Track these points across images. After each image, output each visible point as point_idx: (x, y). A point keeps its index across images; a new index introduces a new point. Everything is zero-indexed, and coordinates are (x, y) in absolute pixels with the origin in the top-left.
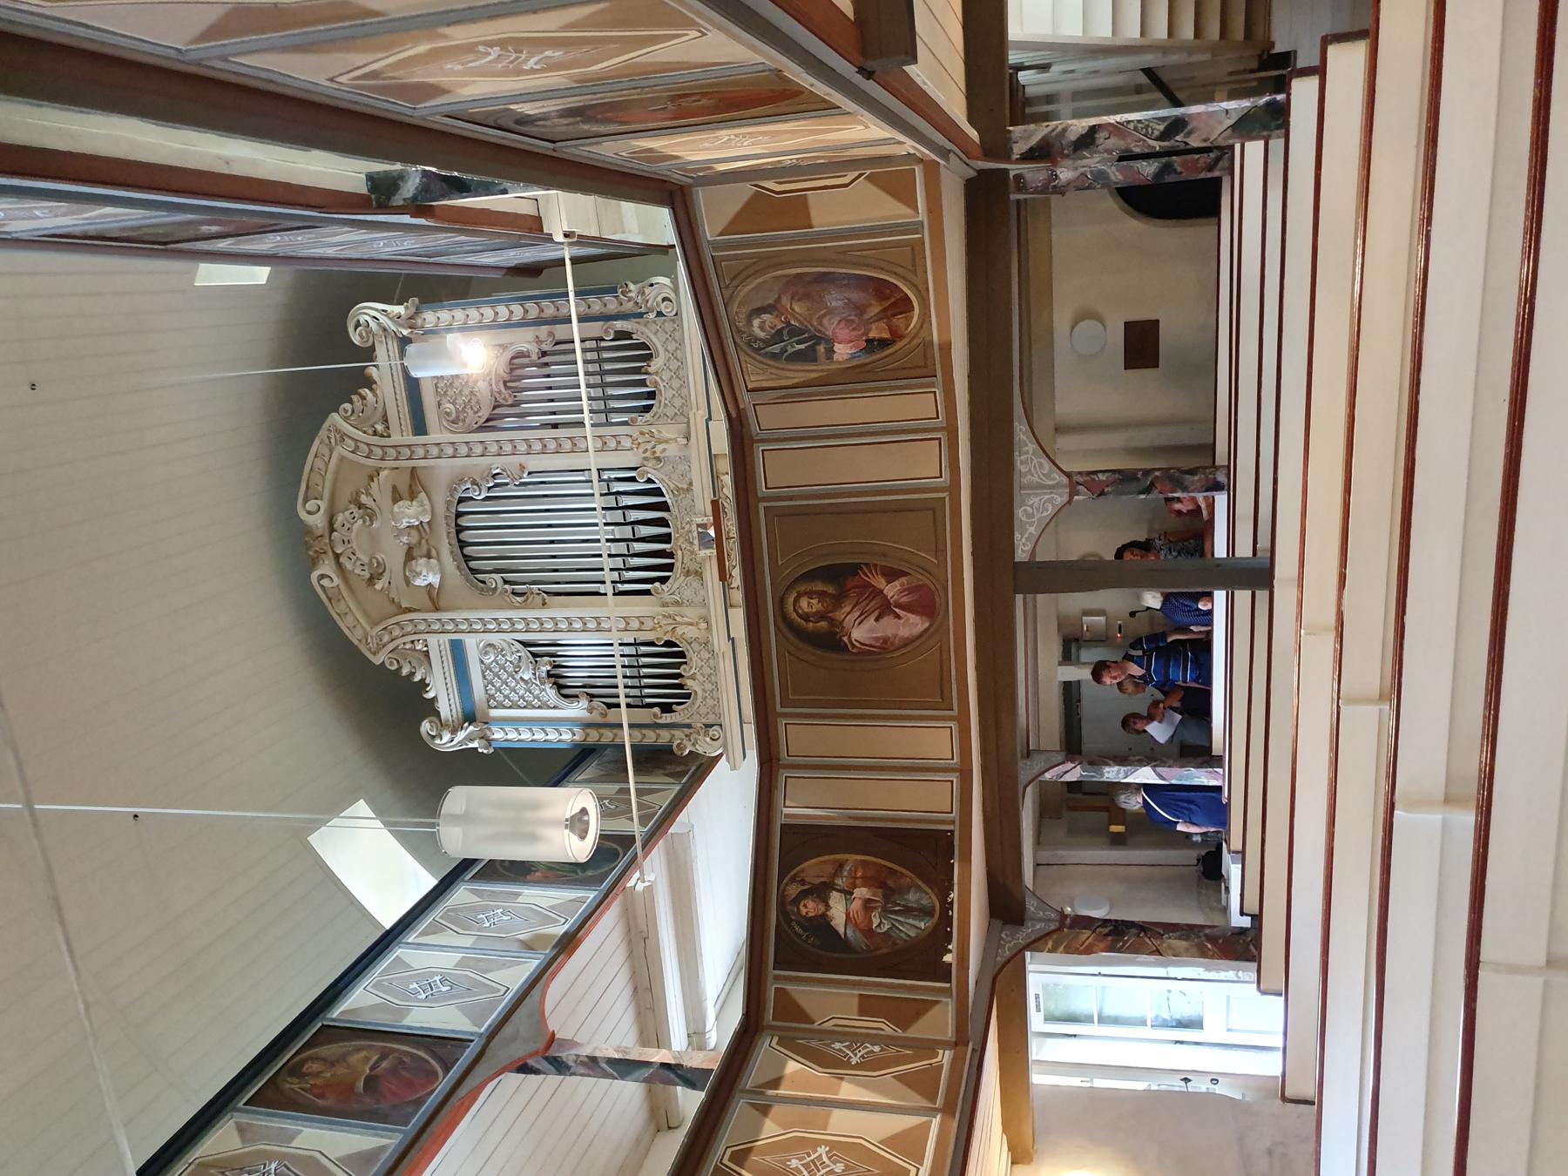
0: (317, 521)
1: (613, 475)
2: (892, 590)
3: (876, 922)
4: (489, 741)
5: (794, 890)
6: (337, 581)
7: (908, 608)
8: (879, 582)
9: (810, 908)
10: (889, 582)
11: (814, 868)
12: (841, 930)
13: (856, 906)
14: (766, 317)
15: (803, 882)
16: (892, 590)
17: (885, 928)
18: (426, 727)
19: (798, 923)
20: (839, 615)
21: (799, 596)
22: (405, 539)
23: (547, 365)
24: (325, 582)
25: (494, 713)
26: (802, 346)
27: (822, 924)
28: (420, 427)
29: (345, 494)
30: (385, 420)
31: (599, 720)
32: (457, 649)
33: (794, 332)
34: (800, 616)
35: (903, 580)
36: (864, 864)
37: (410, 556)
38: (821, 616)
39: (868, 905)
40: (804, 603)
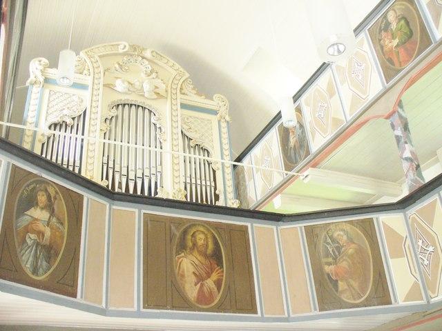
0: (148, 54)
1: (159, 178)
2: (210, 283)
3: (33, 236)
4: (33, 84)
5: (51, 191)
6: (121, 51)
7: (201, 290)
8: (214, 276)
9: (42, 198)
10: (214, 282)
11: (61, 206)
12: (28, 213)
13: (41, 227)
14: (345, 238)
15: (55, 198)
16: (210, 283)
17: (28, 240)
18: (45, 61)
19: (34, 188)
20: (196, 253)
21: (206, 235)
22: (138, 84)
23: (204, 164)
24: (122, 46)
25: (47, 92)
26: (331, 252)
27: (31, 202)
28: (184, 106)
29: (156, 68)
30: (184, 94)
31: (37, 139)
32: (84, 87)
33: (338, 249)
34: (194, 233)
35: (216, 289)
36: (62, 237)
37: (129, 83)
38: (195, 245)
39: (41, 234)
40: (202, 236)
